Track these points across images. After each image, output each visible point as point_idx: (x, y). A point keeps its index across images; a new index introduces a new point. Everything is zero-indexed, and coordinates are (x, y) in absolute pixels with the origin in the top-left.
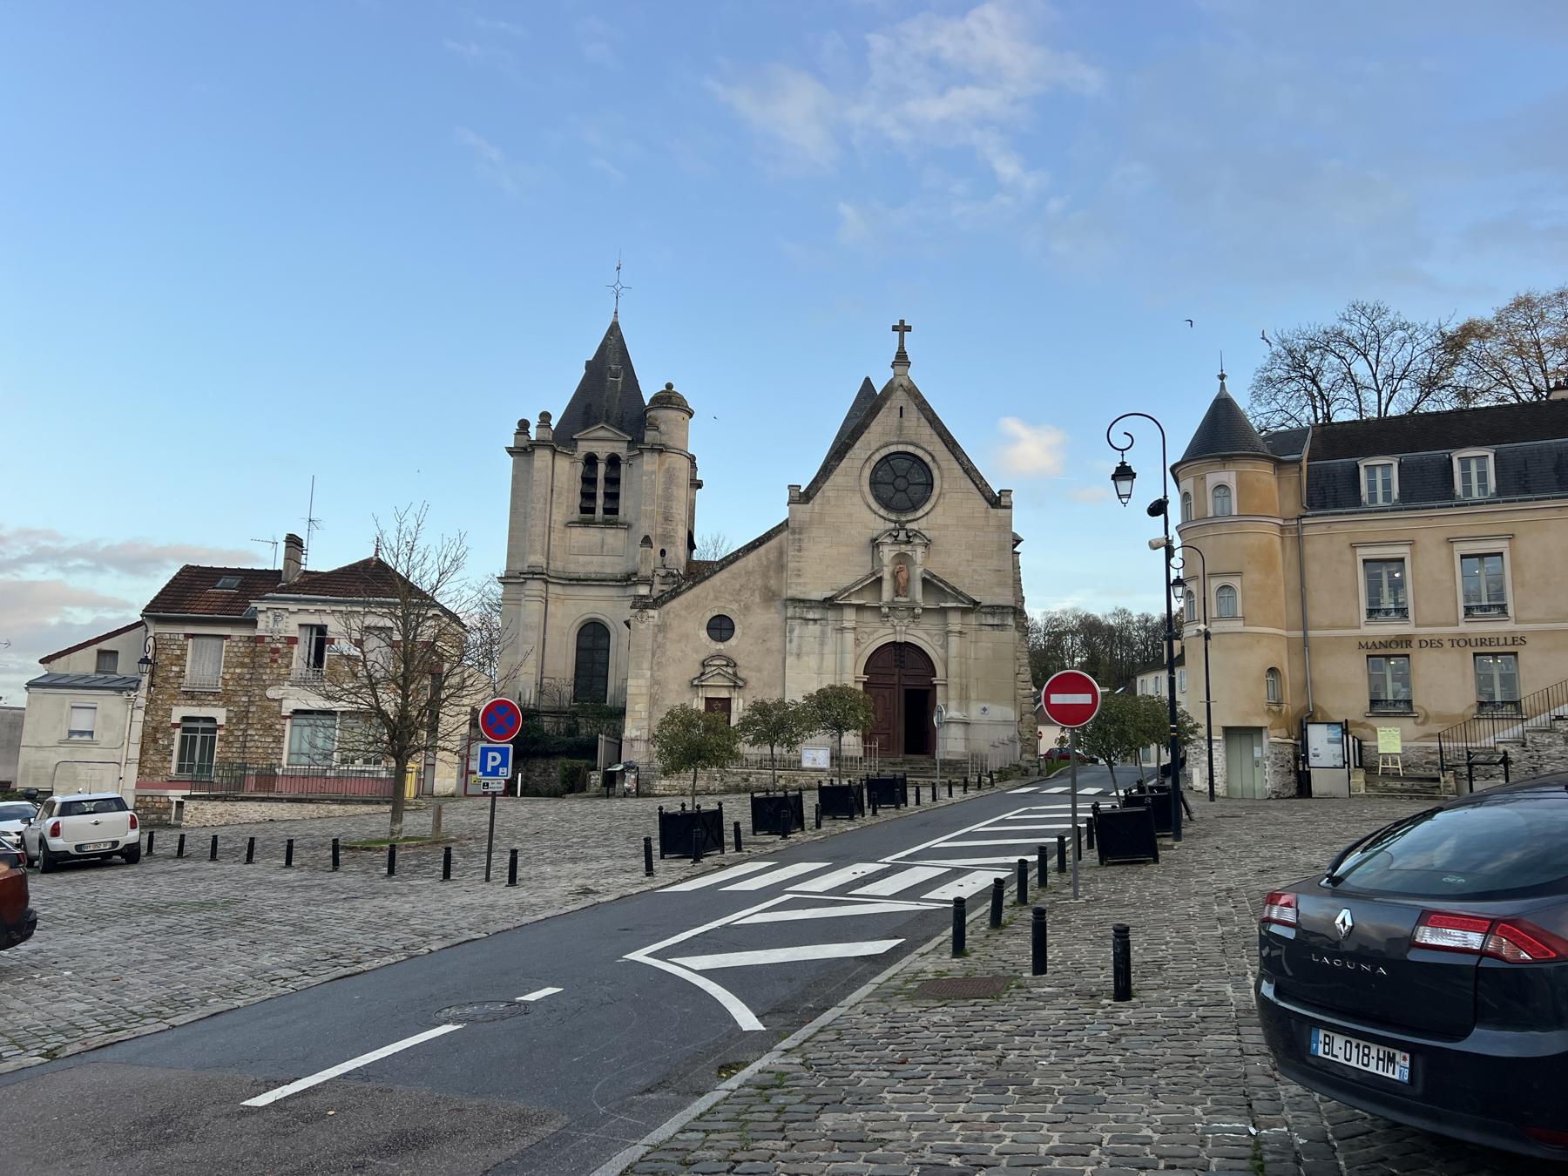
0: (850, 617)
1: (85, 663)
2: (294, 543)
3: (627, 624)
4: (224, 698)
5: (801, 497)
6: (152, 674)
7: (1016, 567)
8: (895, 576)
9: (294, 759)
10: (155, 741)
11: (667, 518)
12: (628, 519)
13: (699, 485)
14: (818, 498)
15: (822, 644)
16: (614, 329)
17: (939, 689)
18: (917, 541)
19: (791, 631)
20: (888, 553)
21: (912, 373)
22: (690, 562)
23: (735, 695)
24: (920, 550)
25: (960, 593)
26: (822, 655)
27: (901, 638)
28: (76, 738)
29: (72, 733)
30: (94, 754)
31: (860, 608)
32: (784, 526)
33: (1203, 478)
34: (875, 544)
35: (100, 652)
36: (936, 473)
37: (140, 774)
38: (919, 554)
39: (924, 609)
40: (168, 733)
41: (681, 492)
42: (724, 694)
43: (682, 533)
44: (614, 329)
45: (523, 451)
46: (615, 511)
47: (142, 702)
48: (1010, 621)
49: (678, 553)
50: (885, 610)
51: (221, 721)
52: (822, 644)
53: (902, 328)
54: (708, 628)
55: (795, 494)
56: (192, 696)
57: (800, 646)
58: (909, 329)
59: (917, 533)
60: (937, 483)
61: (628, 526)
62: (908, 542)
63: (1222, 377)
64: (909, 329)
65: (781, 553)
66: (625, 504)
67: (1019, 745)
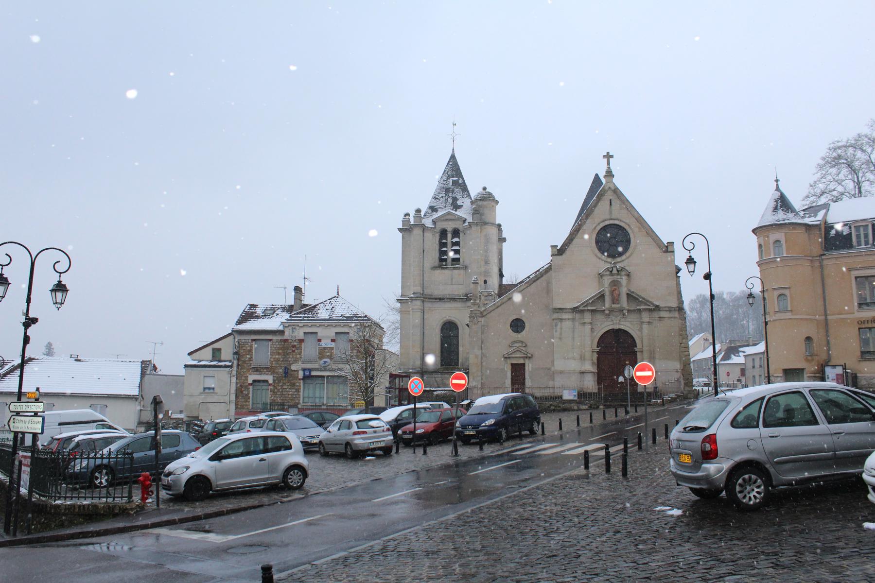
0: (588, 317)
1: (208, 353)
2: (298, 290)
3: (468, 325)
4: (270, 370)
5: (559, 252)
6: (238, 360)
7: (678, 285)
8: (612, 292)
9: (306, 400)
10: (242, 392)
11: (487, 262)
13: (504, 240)
14: (568, 252)
15: (573, 332)
16: (453, 157)
17: (639, 354)
18: (623, 273)
19: (556, 326)
20: (607, 280)
21: (615, 180)
22: (501, 285)
23: (527, 362)
24: (624, 278)
25: (648, 301)
26: (573, 338)
27: (617, 327)
28: (207, 391)
29: (205, 389)
30: (215, 399)
31: (592, 311)
32: (549, 269)
33: (768, 237)
34: (601, 276)
35: (214, 349)
36: (631, 236)
37: (236, 408)
38: (624, 280)
39: (628, 311)
40: (247, 388)
41: (494, 248)
42: (521, 361)
43: (496, 270)
44: (453, 157)
45: (406, 230)
47: (234, 373)
48: (676, 314)
49: (494, 282)
50: (607, 312)
51: (271, 382)
52: (573, 332)
53: (608, 157)
54: (511, 326)
55: (555, 250)
56: (257, 370)
57: (561, 334)
58: (612, 157)
59: (623, 269)
60: (632, 240)
62: (618, 274)
63: (777, 181)
64: (612, 157)
65: (549, 283)
67: (683, 382)
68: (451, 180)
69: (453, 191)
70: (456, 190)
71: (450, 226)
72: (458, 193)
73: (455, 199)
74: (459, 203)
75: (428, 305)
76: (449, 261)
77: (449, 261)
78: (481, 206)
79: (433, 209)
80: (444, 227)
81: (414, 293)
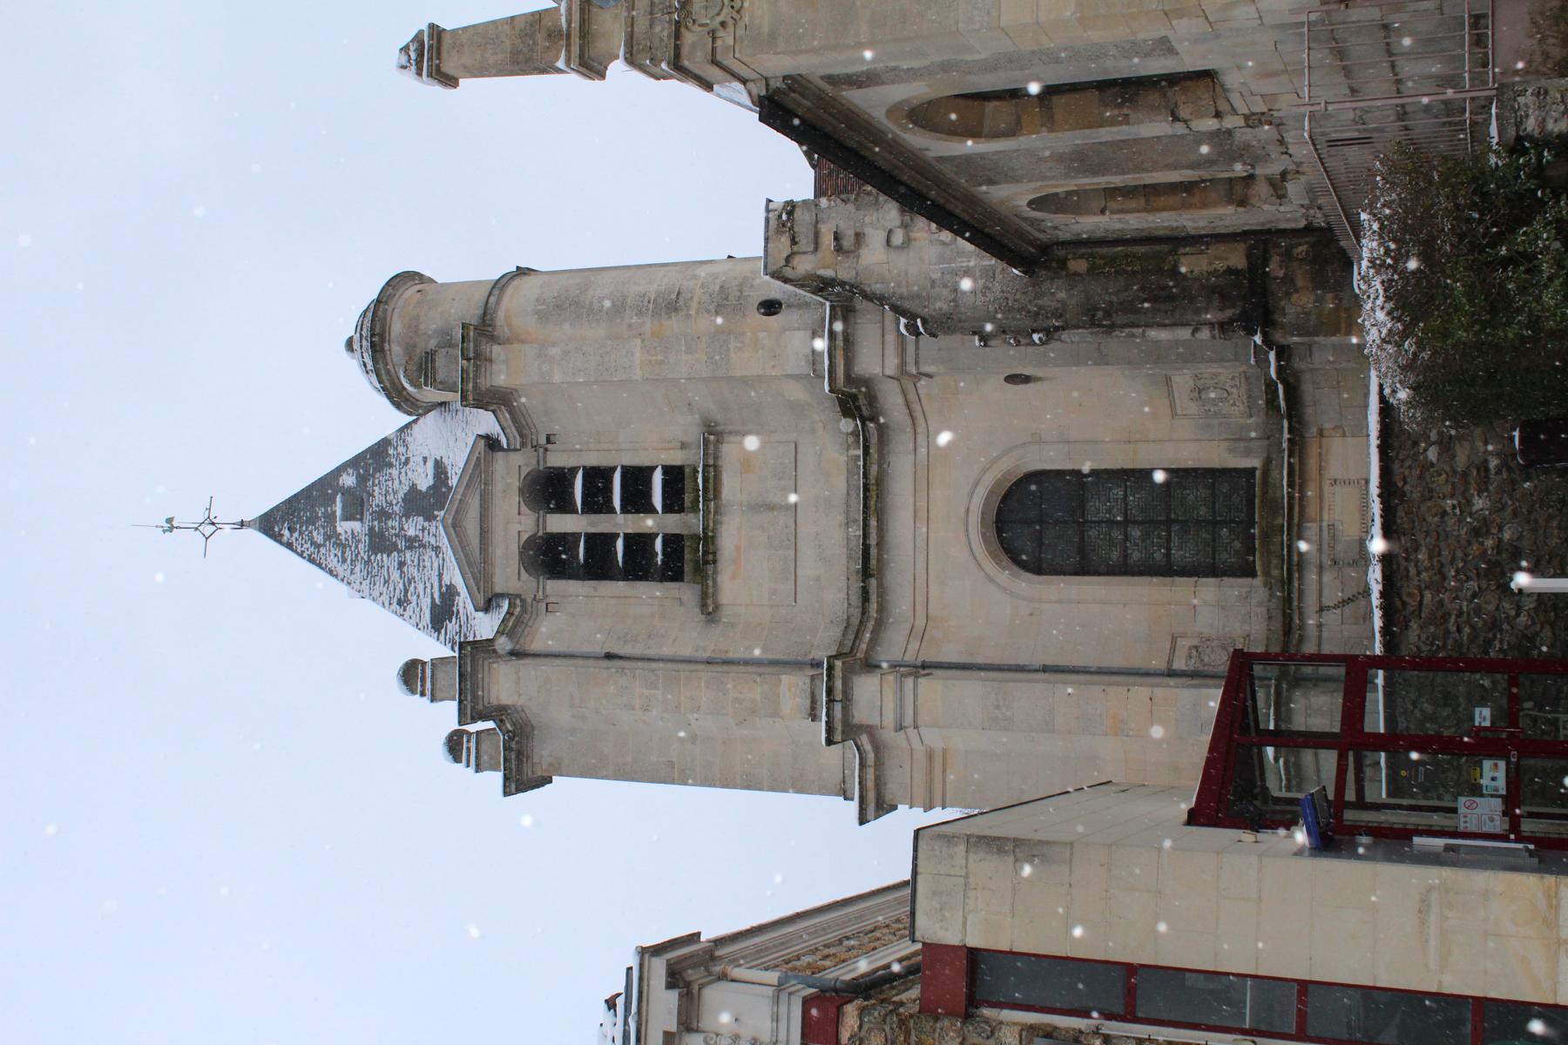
12: (694, 434)
16: (269, 524)
44: (269, 524)
45: (518, 756)
46: (675, 476)
61: (713, 435)
66: (655, 443)
68: (344, 527)
69: (383, 515)
70: (378, 499)
71: (515, 523)
72: (390, 488)
73: (417, 503)
74: (425, 482)
75: (895, 645)
76: (674, 523)
77: (674, 523)
78: (409, 349)
79: (442, 614)
80: (514, 549)
81: (814, 717)
